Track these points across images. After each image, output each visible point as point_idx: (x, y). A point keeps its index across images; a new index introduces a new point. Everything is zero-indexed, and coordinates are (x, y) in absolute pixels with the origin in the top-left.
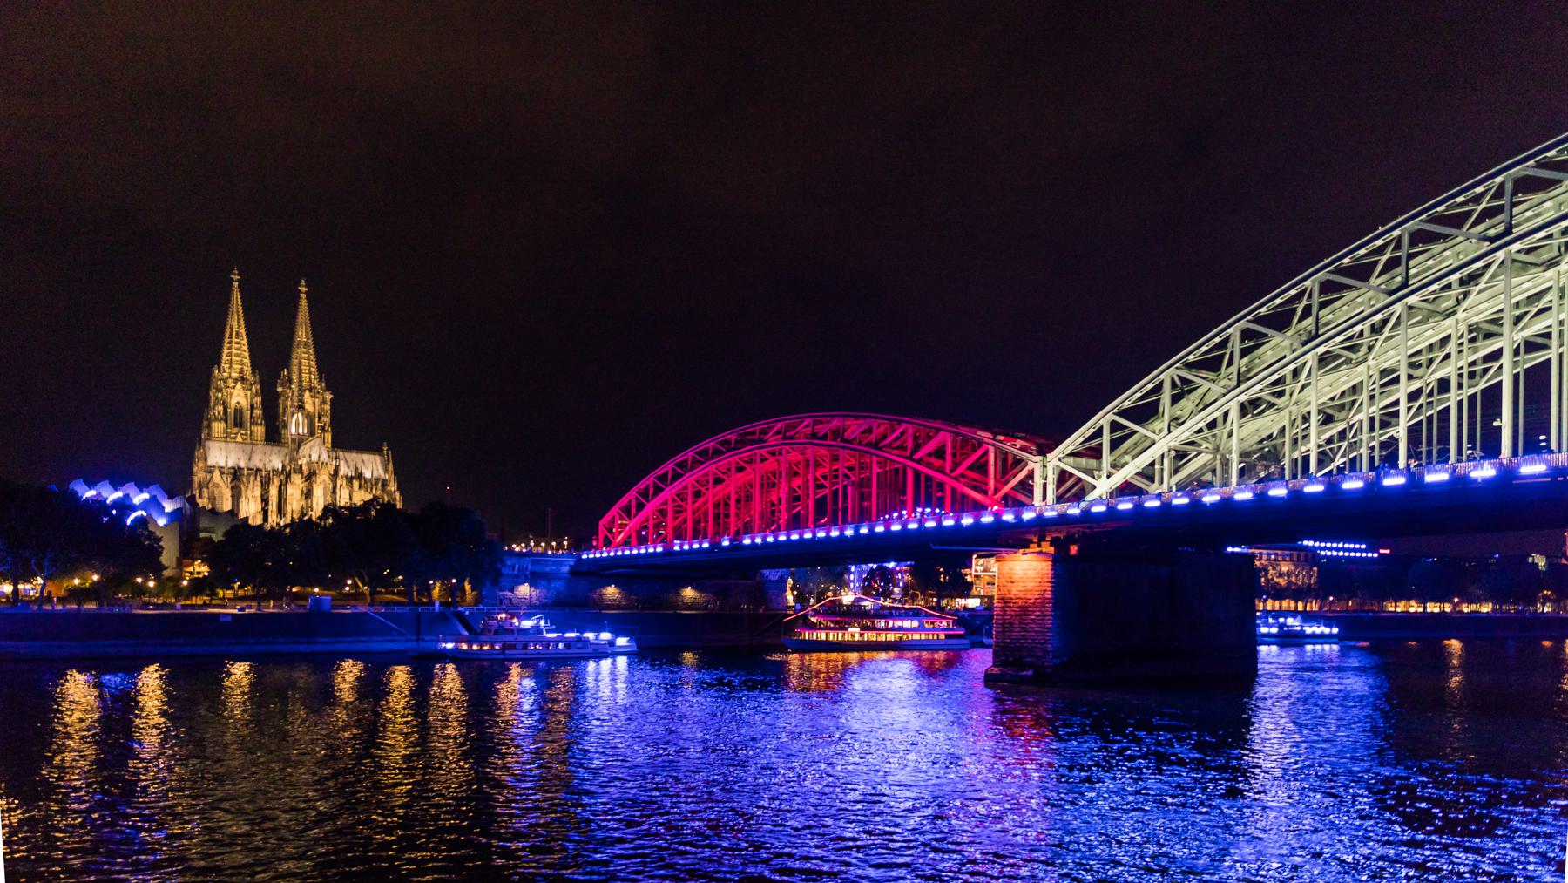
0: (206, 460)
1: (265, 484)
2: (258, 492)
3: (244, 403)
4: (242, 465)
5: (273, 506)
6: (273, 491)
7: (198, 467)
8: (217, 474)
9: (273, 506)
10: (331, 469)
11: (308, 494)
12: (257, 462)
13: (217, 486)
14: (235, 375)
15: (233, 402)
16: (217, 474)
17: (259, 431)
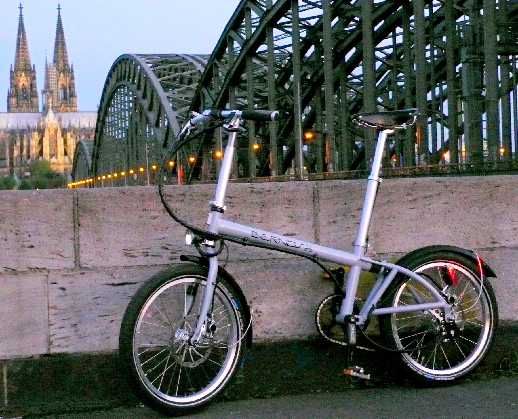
2: (18, 144)
5: (25, 152)
9: (25, 152)
11: (41, 142)
15: (21, 85)
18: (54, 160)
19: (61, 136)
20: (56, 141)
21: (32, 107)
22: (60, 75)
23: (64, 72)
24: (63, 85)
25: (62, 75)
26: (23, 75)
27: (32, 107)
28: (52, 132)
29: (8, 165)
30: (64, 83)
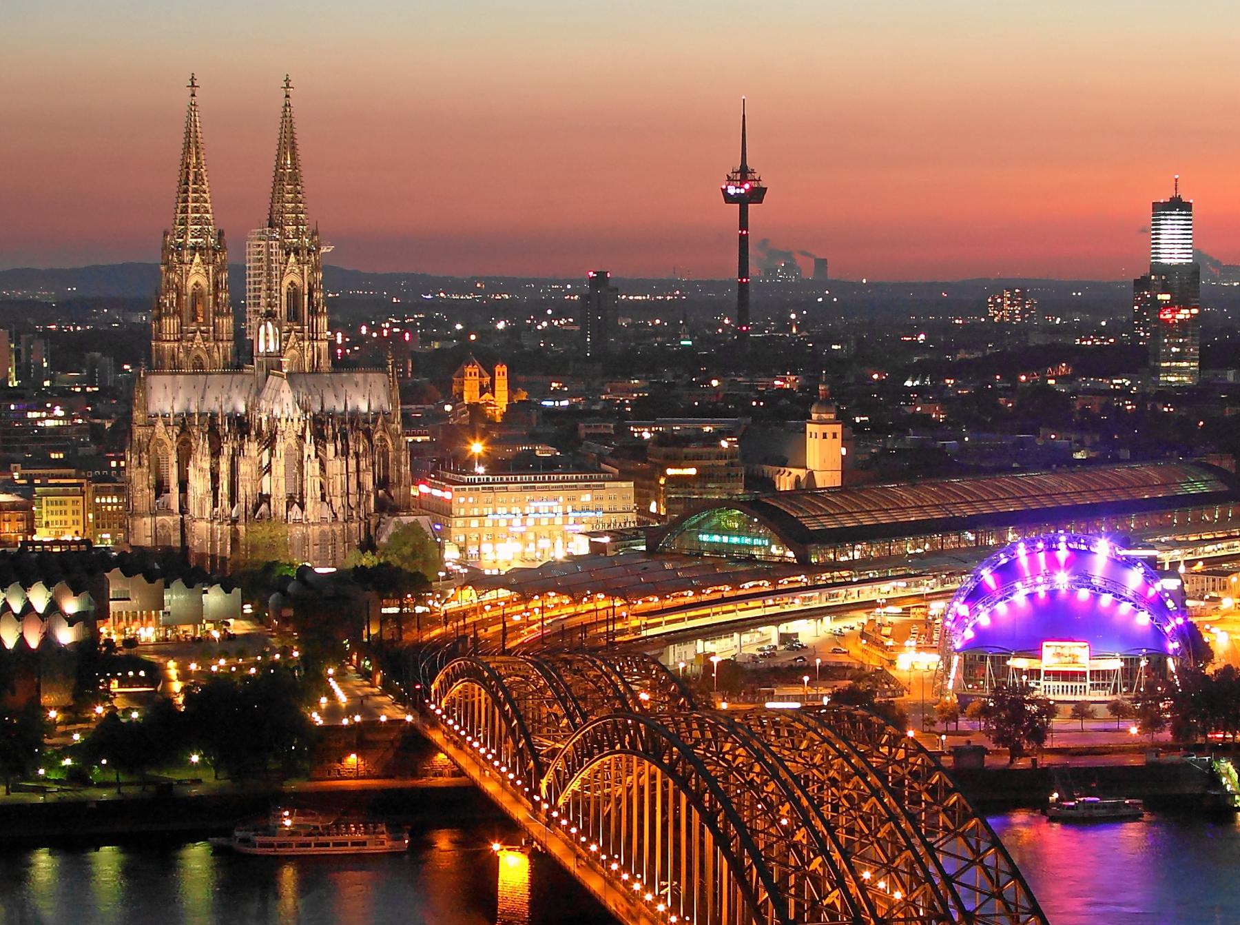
0: (146, 408)
1: (216, 453)
2: (207, 466)
3: (203, 282)
4: (193, 409)
5: (224, 488)
6: (224, 466)
7: (138, 415)
8: (160, 424)
9: (224, 488)
10: (297, 427)
12: (212, 405)
13: (161, 443)
14: (191, 241)
15: (191, 283)
16: (160, 424)
17: (227, 323)
18: (295, 511)
19: (313, 455)
20: (301, 463)
21: (216, 340)
22: (287, 261)
23: (297, 254)
24: (292, 283)
25: (292, 259)
26: (197, 259)
27: (216, 340)
28: (292, 441)
29: (175, 506)
30: (297, 280)
